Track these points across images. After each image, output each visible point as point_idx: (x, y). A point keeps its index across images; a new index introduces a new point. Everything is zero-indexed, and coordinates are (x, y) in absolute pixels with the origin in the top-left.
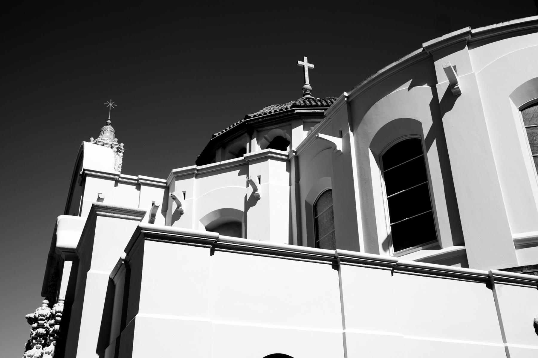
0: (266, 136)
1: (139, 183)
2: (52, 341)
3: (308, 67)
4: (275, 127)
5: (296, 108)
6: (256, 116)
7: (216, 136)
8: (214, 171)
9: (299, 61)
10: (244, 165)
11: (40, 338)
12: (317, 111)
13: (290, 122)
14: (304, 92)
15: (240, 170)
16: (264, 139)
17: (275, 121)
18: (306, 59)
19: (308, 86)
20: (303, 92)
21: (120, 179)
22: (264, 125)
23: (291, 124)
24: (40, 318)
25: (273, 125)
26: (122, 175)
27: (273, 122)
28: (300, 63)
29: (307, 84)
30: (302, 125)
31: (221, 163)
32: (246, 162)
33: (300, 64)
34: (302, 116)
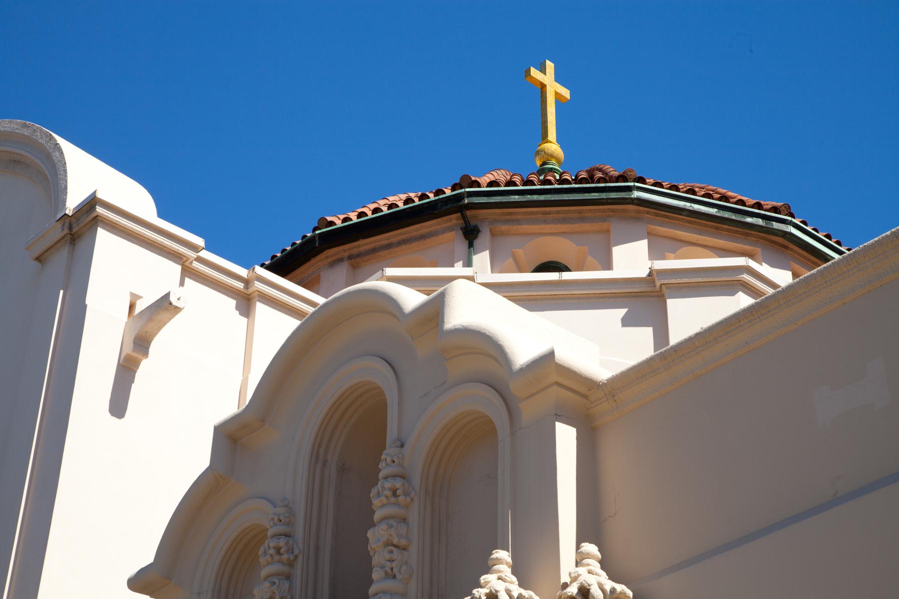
0: (520, 252)
1: (251, 290)
3: (557, 94)
4: (553, 231)
6: (498, 185)
7: (332, 223)
8: (530, 300)
9: (532, 68)
10: (643, 296)
12: (697, 207)
13: (605, 225)
14: (538, 163)
15: (625, 310)
16: (511, 260)
17: (558, 212)
18: (550, 65)
19: (553, 147)
21: (196, 265)
22: (519, 217)
23: (608, 231)
25: (548, 224)
26: (205, 254)
27: (549, 213)
28: (535, 73)
29: (551, 142)
30: (644, 243)
31: (564, 278)
32: (649, 289)
34: (648, 213)
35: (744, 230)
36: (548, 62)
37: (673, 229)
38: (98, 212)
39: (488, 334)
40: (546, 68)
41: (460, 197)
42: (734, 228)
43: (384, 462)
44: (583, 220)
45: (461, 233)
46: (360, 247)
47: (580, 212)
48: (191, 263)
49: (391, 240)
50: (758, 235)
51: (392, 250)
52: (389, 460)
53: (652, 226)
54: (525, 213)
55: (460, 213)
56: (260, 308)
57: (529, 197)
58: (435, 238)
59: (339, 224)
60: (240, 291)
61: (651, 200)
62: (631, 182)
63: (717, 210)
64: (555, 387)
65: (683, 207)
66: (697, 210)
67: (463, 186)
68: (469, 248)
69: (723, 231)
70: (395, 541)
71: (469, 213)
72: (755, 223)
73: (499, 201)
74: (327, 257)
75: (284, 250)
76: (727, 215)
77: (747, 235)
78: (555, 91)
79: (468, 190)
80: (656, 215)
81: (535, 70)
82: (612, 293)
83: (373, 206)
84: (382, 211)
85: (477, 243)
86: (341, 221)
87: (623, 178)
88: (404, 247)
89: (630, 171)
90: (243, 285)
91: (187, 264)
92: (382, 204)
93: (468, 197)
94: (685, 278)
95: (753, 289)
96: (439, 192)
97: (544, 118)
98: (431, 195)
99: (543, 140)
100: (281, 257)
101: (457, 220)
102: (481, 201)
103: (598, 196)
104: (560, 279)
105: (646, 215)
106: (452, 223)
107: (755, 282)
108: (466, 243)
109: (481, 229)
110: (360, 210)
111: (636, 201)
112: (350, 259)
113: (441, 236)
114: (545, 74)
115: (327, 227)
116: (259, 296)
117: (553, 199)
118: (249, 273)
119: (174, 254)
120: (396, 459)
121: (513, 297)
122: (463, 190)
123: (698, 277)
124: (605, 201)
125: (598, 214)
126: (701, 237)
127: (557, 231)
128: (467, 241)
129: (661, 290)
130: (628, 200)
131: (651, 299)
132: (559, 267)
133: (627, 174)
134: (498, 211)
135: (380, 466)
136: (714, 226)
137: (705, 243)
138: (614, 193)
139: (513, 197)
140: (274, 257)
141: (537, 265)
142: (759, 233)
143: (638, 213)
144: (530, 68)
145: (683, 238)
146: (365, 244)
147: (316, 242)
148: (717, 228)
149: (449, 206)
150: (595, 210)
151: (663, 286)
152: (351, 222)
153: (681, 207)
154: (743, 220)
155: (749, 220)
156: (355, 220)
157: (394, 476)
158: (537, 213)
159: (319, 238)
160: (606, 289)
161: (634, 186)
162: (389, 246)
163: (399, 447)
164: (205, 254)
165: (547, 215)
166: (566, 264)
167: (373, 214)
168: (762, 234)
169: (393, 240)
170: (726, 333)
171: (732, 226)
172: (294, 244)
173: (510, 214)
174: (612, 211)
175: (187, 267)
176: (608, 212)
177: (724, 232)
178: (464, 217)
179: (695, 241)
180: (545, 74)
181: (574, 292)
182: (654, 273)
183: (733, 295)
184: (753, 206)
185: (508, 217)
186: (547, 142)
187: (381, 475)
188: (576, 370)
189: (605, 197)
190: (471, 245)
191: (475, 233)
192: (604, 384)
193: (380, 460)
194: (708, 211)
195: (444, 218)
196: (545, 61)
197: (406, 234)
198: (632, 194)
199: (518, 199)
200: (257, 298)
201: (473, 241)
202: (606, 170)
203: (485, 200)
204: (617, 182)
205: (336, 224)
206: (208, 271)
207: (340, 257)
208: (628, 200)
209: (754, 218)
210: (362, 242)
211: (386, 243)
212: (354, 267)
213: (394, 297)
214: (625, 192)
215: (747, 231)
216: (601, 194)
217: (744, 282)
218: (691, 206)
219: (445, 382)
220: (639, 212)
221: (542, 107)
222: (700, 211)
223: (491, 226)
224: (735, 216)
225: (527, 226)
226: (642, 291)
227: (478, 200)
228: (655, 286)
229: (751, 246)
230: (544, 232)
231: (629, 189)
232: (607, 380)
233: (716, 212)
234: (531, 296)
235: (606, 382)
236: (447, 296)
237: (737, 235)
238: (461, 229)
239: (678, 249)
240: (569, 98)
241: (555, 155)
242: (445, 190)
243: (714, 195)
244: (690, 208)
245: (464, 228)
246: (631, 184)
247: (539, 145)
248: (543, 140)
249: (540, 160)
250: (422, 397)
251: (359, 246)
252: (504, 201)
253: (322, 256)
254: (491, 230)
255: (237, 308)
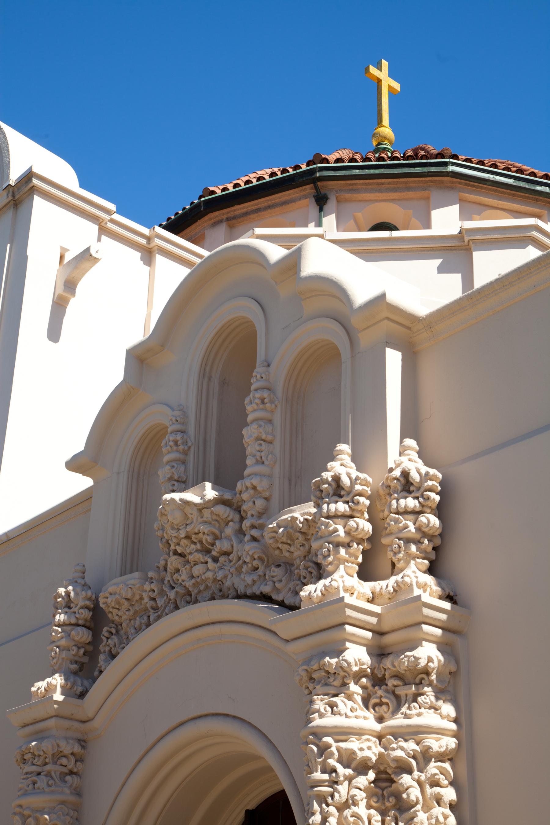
0: (359, 215)
1: (152, 245)
2: (411, 557)
3: (390, 87)
4: (385, 198)
5: (452, 160)
6: (343, 161)
7: (213, 192)
8: (367, 253)
9: (371, 66)
10: (455, 250)
11: (358, 544)
12: (498, 178)
13: (426, 193)
14: (375, 143)
15: (441, 260)
16: (352, 221)
18: (385, 64)
19: (386, 130)
20: (373, 145)
21: (110, 225)
22: (359, 187)
23: (428, 198)
24: (358, 487)
25: (381, 192)
26: (116, 217)
27: (383, 184)
28: (373, 70)
29: (384, 126)
30: (456, 207)
33: (373, 73)
34: (460, 183)
35: (535, 197)
36: (383, 61)
37: (479, 196)
38: (34, 183)
39: (334, 280)
40: (381, 66)
41: (313, 171)
42: (527, 195)
43: (255, 377)
44: (409, 189)
45: (313, 200)
46: (235, 211)
47: (406, 183)
48: (106, 223)
49: (259, 206)
50: (545, 200)
51: (260, 213)
52: (258, 376)
53: (463, 194)
54: (363, 184)
55: (313, 184)
56: (159, 259)
57: (367, 171)
58: (293, 204)
59: (219, 193)
60: (143, 246)
61: (463, 173)
62: (447, 158)
63: (514, 180)
64: (386, 321)
65: (488, 178)
66: (498, 181)
67: (315, 162)
68: (320, 212)
69: (518, 197)
70: (264, 437)
71: (320, 184)
72: (544, 191)
73: (343, 174)
74: (210, 219)
75: (177, 214)
76: (521, 184)
77: (537, 200)
78: (389, 85)
79: (319, 165)
80: (466, 185)
81: (373, 67)
82: (430, 247)
83: (245, 179)
84: (252, 182)
85: (326, 208)
86: (220, 191)
87: (441, 155)
88: (269, 211)
89: (447, 150)
90: (146, 241)
91: (103, 224)
92: (252, 177)
93: (319, 171)
94: (488, 235)
95: (540, 243)
96: (297, 167)
97: (380, 107)
98: (291, 170)
99: (379, 124)
100: (175, 219)
101: (310, 190)
102: (330, 175)
103: (421, 170)
104: (391, 236)
105: (458, 185)
106: (307, 192)
107: (542, 238)
108: (317, 208)
109: (329, 197)
110: (235, 182)
111: (450, 174)
112: (227, 221)
113: (298, 202)
114: (381, 71)
115: (209, 195)
116: (158, 249)
117: (385, 173)
118: (150, 231)
119: (92, 217)
120: (263, 376)
121: (354, 251)
122: (315, 166)
123: (498, 234)
124: (426, 174)
125: (421, 184)
126: (501, 202)
127: (388, 198)
128: (319, 206)
129: (469, 244)
130: (445, 173)
131: (461, 251)
132: (389, 227)
133: (444, 152)
134: (342, 182)
135: (252, 381)
136: (511, 193)
137: (504, 207)
138: (433, 168)
139: (354, 171)
140: (169, 219)
141: (372, 225)
142: (546, 199)
143: (452, 184)
144: (369, 66)
145: (487, 203)
146: (239, 209)
147: (201, 208)
148: (513, 195)
149: (305, 179)
150: (418, 181)
151: (470, 241)
152: (228, 192)
153: (486, 178)
154: (534, 188)
155: (539, 188)
156: (231, 190)
157: (262, 389)
158: (373, 184)
159: (203, 204)
160: (427, 244)
161: (450, 162)
162: (258, 211)
163: (266, 367)
164: (116, 217)
165: (380, 186)
166: (395, 224)
167: (245, 185)
168: (548, 199)
169: (261, 206)
170: (519, 279)
171: (525, 193)
172: (184, 209)
173: (352, 184)
174: (432, 182)
175: (103, 227)
176: (429, 183)
177: (519, 198)
178: (316, 188)
179: (495, 206)
180: (381, 71)
181: (401, 247)
182: (464, 231)
183: (524, 247)
184: (542, 177)
185: (350, 187)
186: (382, 127)
187: (253, 387)
188: (402, 308)
189: (426, 171)
190: (321, 209)
191: (325, 200)
192: (423, 318)
193: (252, 376)
194: (507, 182)
195: (300, 188)
196: (381, 60)
197: (270, 201)
198: (448, 168)
199: (358, 172)
200: (157, 251)
201: (323, 207)
202: (428, 149)
203: (333, 174)
204: (436, 158)
205: (216, 193)
206: (119, 230)
207: (220, 219)
208: (445, 173)
209: (543, 187)
210: (237, 207)
211: (256, 208)
212: (231, 227)
213: (262, 251)
214: (443, 166)
215: (537, 197)
216: (423, 168)
217: (534, 238)
218: (494, 177)
219: (301, 317)
220: (453, 182)
221: (378, 97)
222: (500, 181)
223: (337, 194)
224: (528, 185)
225: (365, 194)
226: (454, 245)
227: (327, 174)
228: (464, 242)
229: (540, 209)
230: (379, 199)
231: (446, 164)
232: (426, 316)
233: (513, 182)
234: (367, 249)
235: (425, 317)
236: (303, 250)
237: (529, 200)
238: (314, 197)
239: (483, 212)
240: (400, 91)
241: (388, 137)
242: (301, 165)
243: (512, 168)
244: (493, 179)
245: (317, 196)
246: (447, 160)
247: (376, 129)
248: (379, 124)
249: (376, 141)
250: (283, 329)
251: (235, 211)
252: (347, 174)
253: (206, 218)
254: (337, 198)
255: (142, 259)
